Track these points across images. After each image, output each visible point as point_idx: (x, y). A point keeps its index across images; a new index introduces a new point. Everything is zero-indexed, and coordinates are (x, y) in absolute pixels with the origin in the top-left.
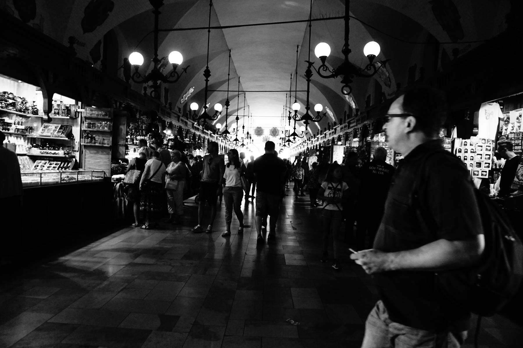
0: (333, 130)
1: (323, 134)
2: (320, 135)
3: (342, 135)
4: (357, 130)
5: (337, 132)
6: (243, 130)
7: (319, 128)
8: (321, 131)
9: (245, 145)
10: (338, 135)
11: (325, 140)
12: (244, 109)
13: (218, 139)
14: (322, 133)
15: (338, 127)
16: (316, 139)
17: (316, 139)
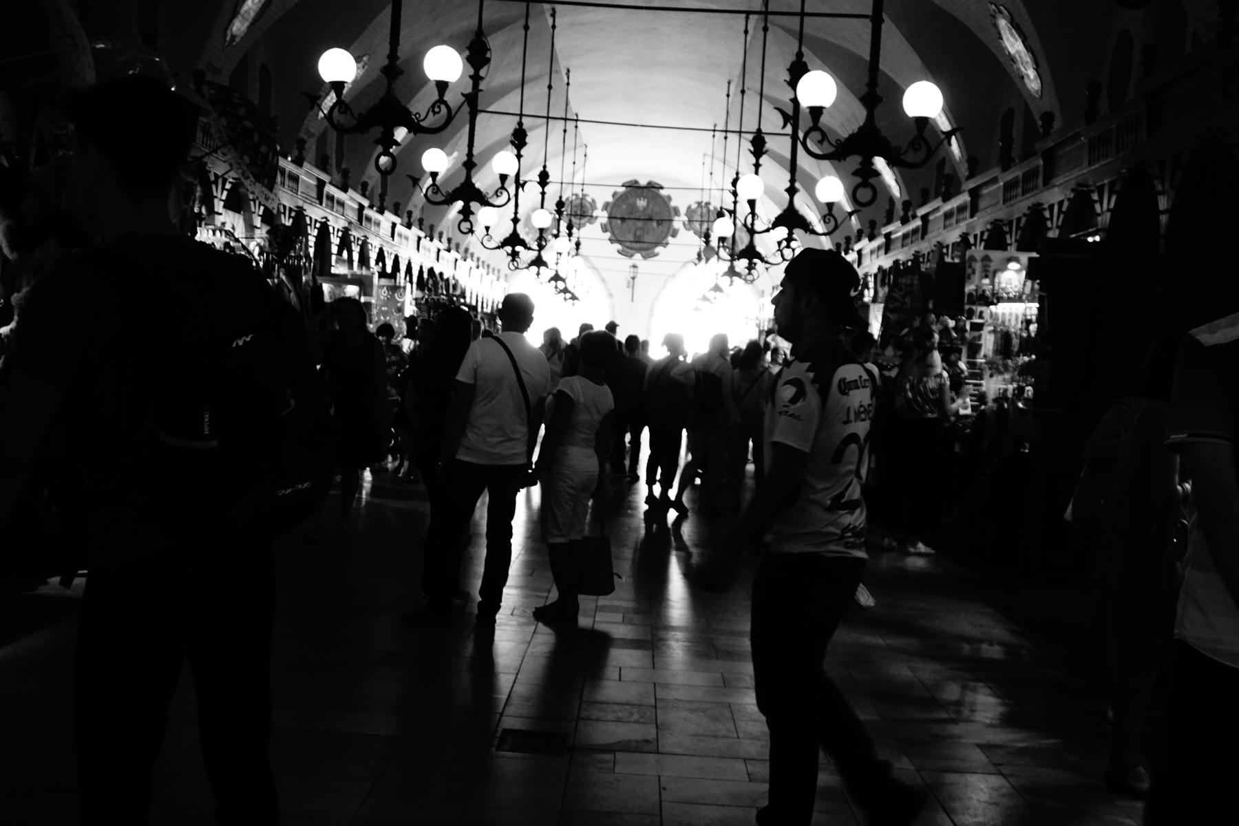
0: (964, 198)
1: (914, 217)
2: (898, 223)
3: (947, 247)
4: (1006, 229)
5: (982, 204)
6: (543, 194)
7: (895, 190)
8: (907, 205)
9: (545, 264)
10: (934, 242)
11: (925, 246)
12: (550, 87)
13: (400, 235)
14: (910, 213)
15: (937, 210)
16: (880, 241)
17: (880, 241)
